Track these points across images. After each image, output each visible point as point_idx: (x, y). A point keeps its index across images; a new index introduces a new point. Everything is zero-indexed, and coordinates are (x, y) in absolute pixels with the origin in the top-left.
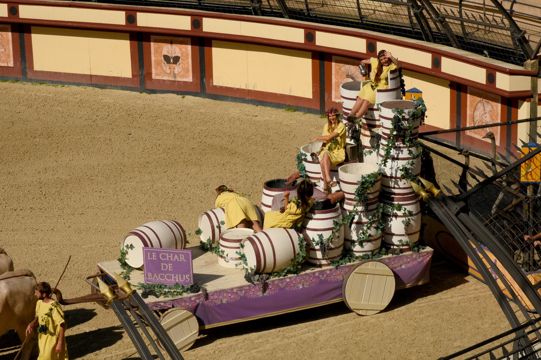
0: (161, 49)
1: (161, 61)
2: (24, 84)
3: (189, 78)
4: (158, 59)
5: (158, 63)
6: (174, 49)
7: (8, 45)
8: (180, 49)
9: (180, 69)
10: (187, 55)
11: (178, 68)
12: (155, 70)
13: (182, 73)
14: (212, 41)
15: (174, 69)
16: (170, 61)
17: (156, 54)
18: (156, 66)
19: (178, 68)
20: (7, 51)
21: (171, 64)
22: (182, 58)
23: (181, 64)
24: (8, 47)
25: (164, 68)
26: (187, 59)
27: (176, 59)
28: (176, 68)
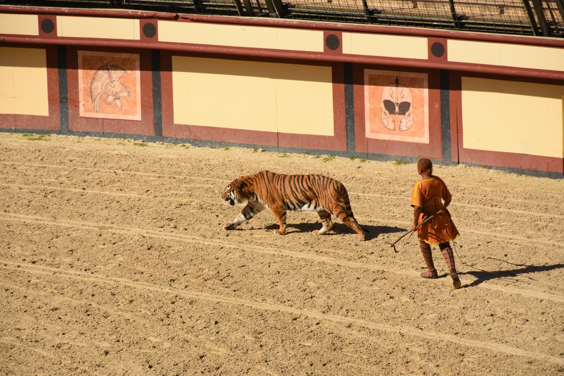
0: (381, 90)
1: (380, 110)
2: (187, 148)
3: (423, 137)
4: (375, 107)
5: (375, 113)
6: (400, 91)
7: (134, 85)
8: (410, 91)
9: (409, 123)
10: (422, 100)
11: (408, 120)
12: (371, 124)
13: (413, 129)
14: (462, 77)
15: (401, 122)
16: (395, 109)
17: (373, 98)
18: (372, 117)
19: (408, 120)
20: (132, 97)
21: (395, 114)
22: (414, 105)
23: (412, 115)
24: (133, 88)
25: (384, 121)
26: (422, 106)
27: (405, 107)
28: (403, 121)
